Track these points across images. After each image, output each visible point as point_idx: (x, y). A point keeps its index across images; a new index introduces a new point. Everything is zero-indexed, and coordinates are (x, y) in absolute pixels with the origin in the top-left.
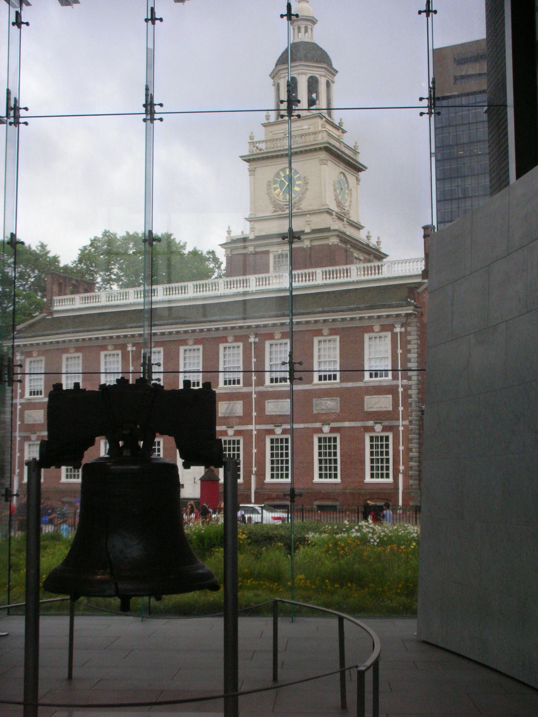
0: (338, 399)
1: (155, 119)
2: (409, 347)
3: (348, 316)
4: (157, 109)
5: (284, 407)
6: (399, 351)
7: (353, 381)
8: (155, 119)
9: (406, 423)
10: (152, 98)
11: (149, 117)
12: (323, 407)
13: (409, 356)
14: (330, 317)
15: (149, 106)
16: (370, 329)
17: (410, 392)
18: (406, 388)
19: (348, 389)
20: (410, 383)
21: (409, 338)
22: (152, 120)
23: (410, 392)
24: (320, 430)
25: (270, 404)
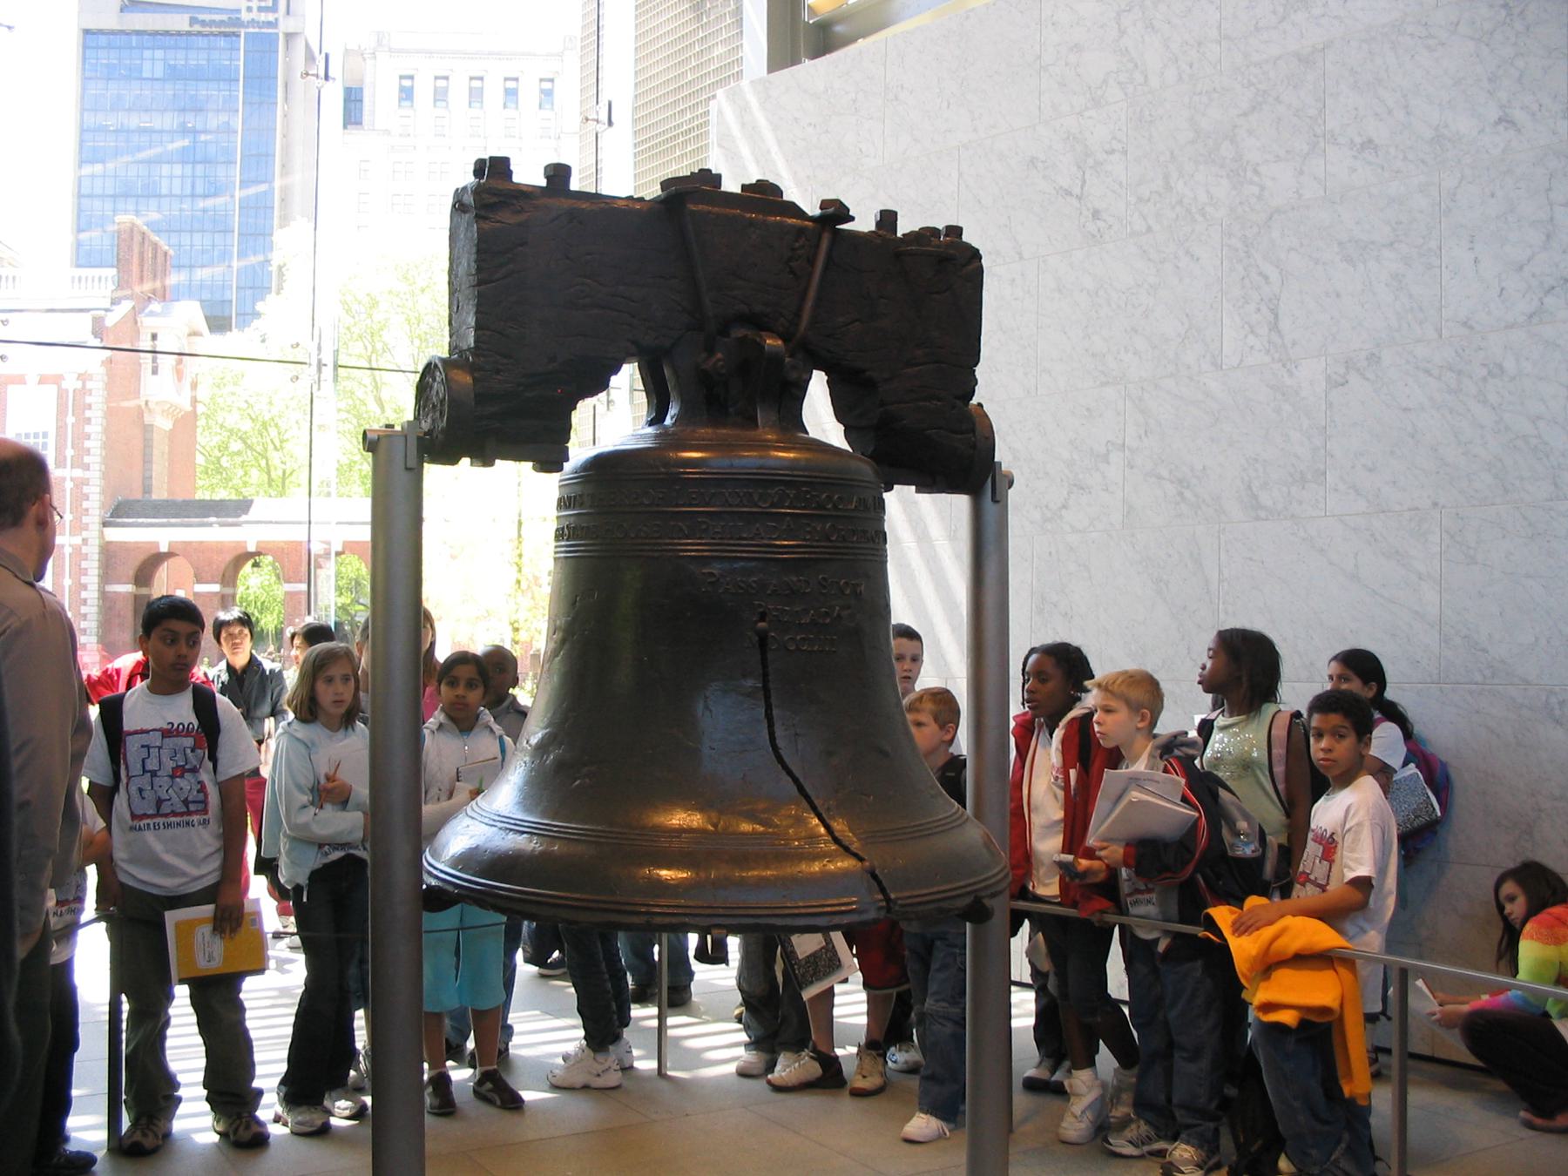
2: (88, 414)
6: (70, 420)
9: (77, 540)
13: (88, 429)
17: (86, 490)
18: (80, 484)
20: (87, 474)
21: (88, 400)
23: (86, 490)
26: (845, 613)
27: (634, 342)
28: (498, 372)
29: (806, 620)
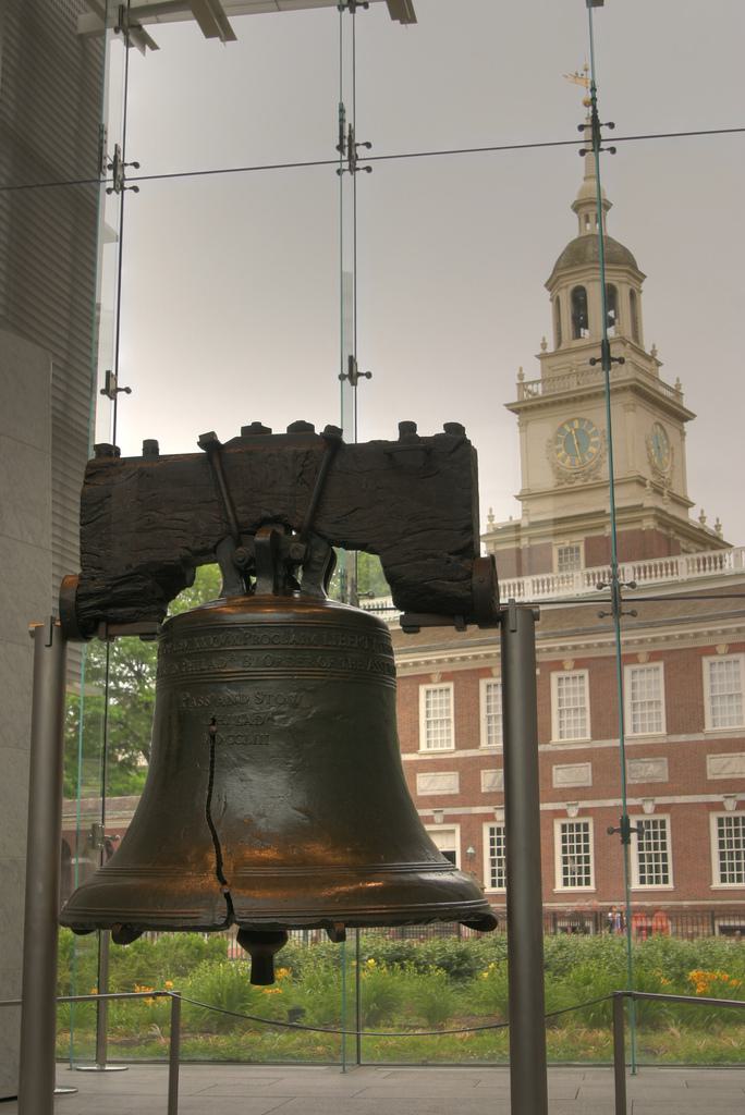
0: (665, 759)
1: (358, 169)
3: (676, 631)
4: (361, 151)
5: (581, 775)
7: (687, 732)
8: (358, 169)
10: (352, 131)
11: (346, 165)
12: (642, 773)
14: (648, 634)
15: (347, 144)
16: (711, 651)
19: (680, 744)
22: (353, 169)
24: (639, 810)
25: (560, 772)
26: (276, 718)
27: (187, 548)
28: (93, 579)
29: (242, 721)
